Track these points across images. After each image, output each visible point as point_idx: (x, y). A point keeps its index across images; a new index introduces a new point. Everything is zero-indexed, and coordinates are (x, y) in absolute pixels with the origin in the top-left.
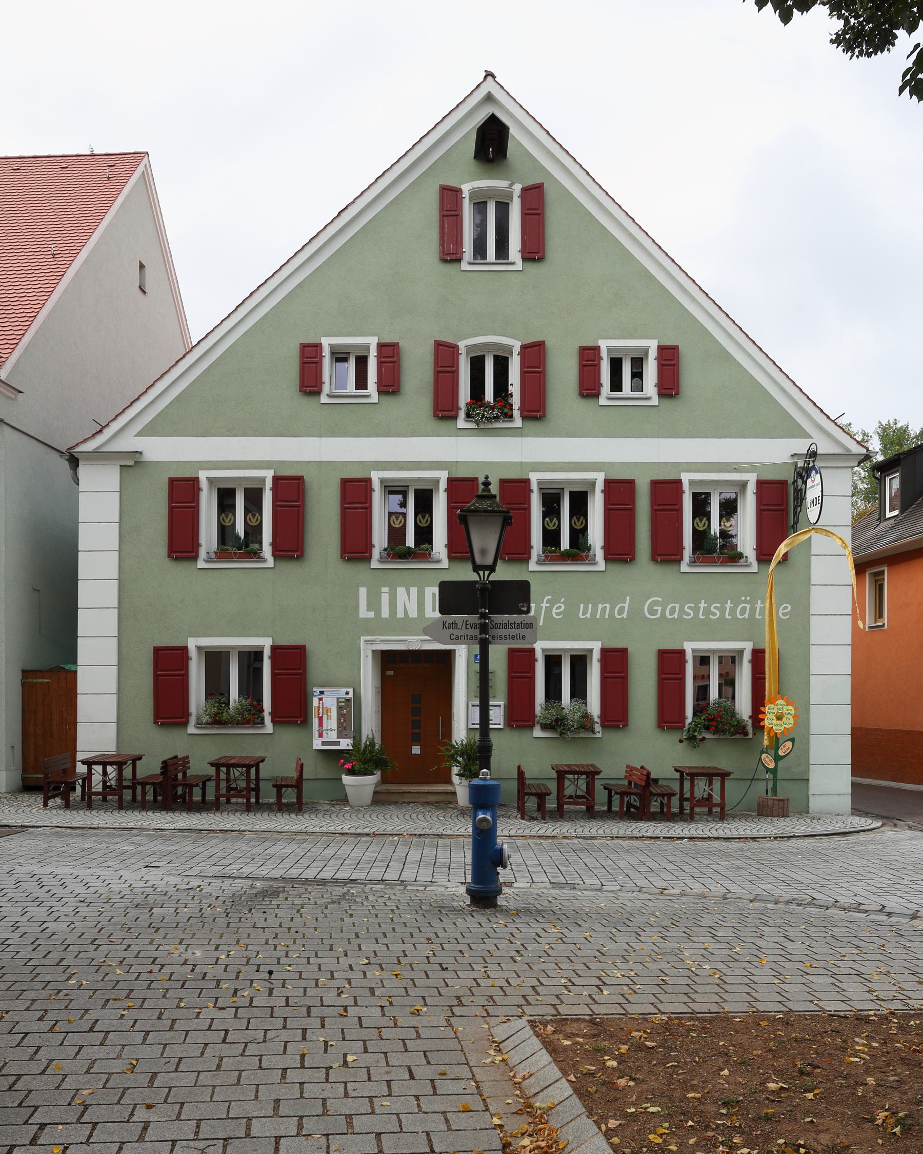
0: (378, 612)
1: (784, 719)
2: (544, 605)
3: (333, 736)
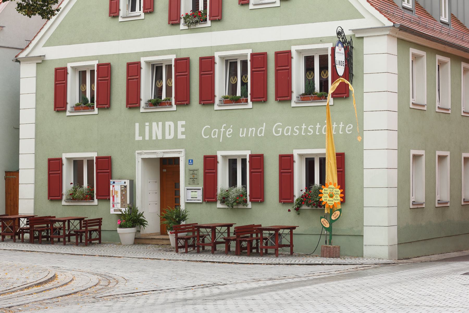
0: (144, 137)
1: (334, 197)
2: (222, 130)
3: (118, 206)
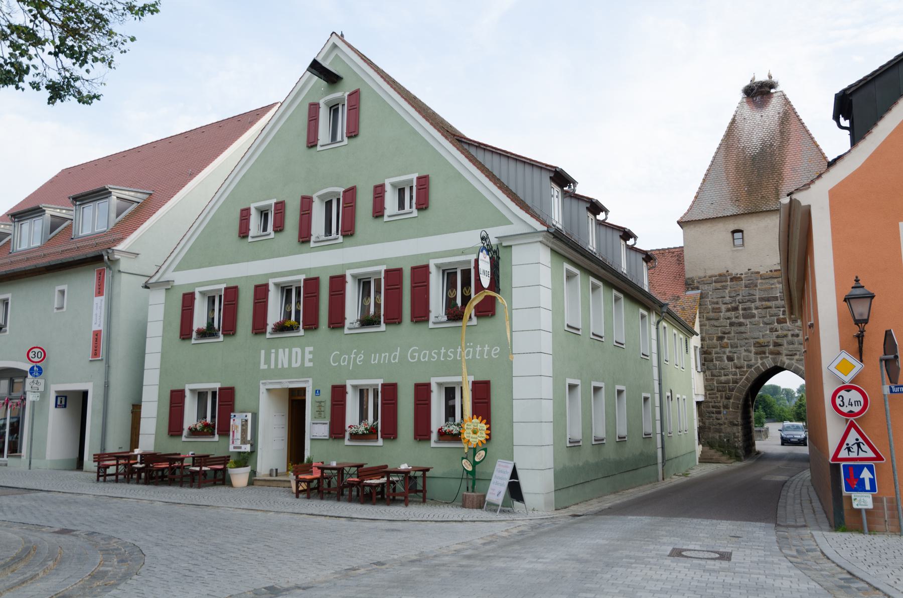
0: (269, 366)
1: (479, 434)
2: (353, 356)
3: (238, 443)
